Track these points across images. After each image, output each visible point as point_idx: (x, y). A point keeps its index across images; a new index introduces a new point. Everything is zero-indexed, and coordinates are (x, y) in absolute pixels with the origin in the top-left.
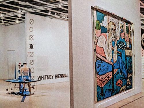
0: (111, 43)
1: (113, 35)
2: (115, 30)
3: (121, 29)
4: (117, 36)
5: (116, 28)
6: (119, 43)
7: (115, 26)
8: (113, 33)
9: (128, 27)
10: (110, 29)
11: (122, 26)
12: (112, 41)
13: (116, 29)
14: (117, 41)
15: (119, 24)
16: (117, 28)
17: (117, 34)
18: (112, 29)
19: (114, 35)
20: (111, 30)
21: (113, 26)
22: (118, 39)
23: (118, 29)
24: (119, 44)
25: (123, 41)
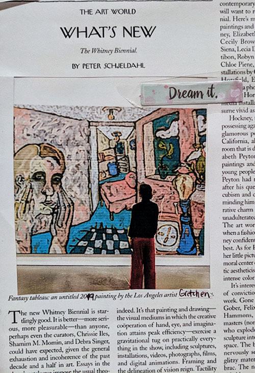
0: (28, 245)
1: (38, 207)
2: (57, 179)
3: (104, 166)
4: (73, 204)
5: (65, 168)
6: (87, 237)
7: (59, 158)
8: (44, 193)
9: (175, 140)
10: (22, 178)
11: (119, 148)
12: (32, 235)
13: (68, 174)
14: (71, 226)
15: (88, 142)
16: (70, 166)
17: (69, 193)
18: (38, 176)
19: (46, 203)
20: (26, 183)
21: (45, 165)
22: (80, 215)
23: (84, 168)
24: (81, 243)
25: (116, 223)
